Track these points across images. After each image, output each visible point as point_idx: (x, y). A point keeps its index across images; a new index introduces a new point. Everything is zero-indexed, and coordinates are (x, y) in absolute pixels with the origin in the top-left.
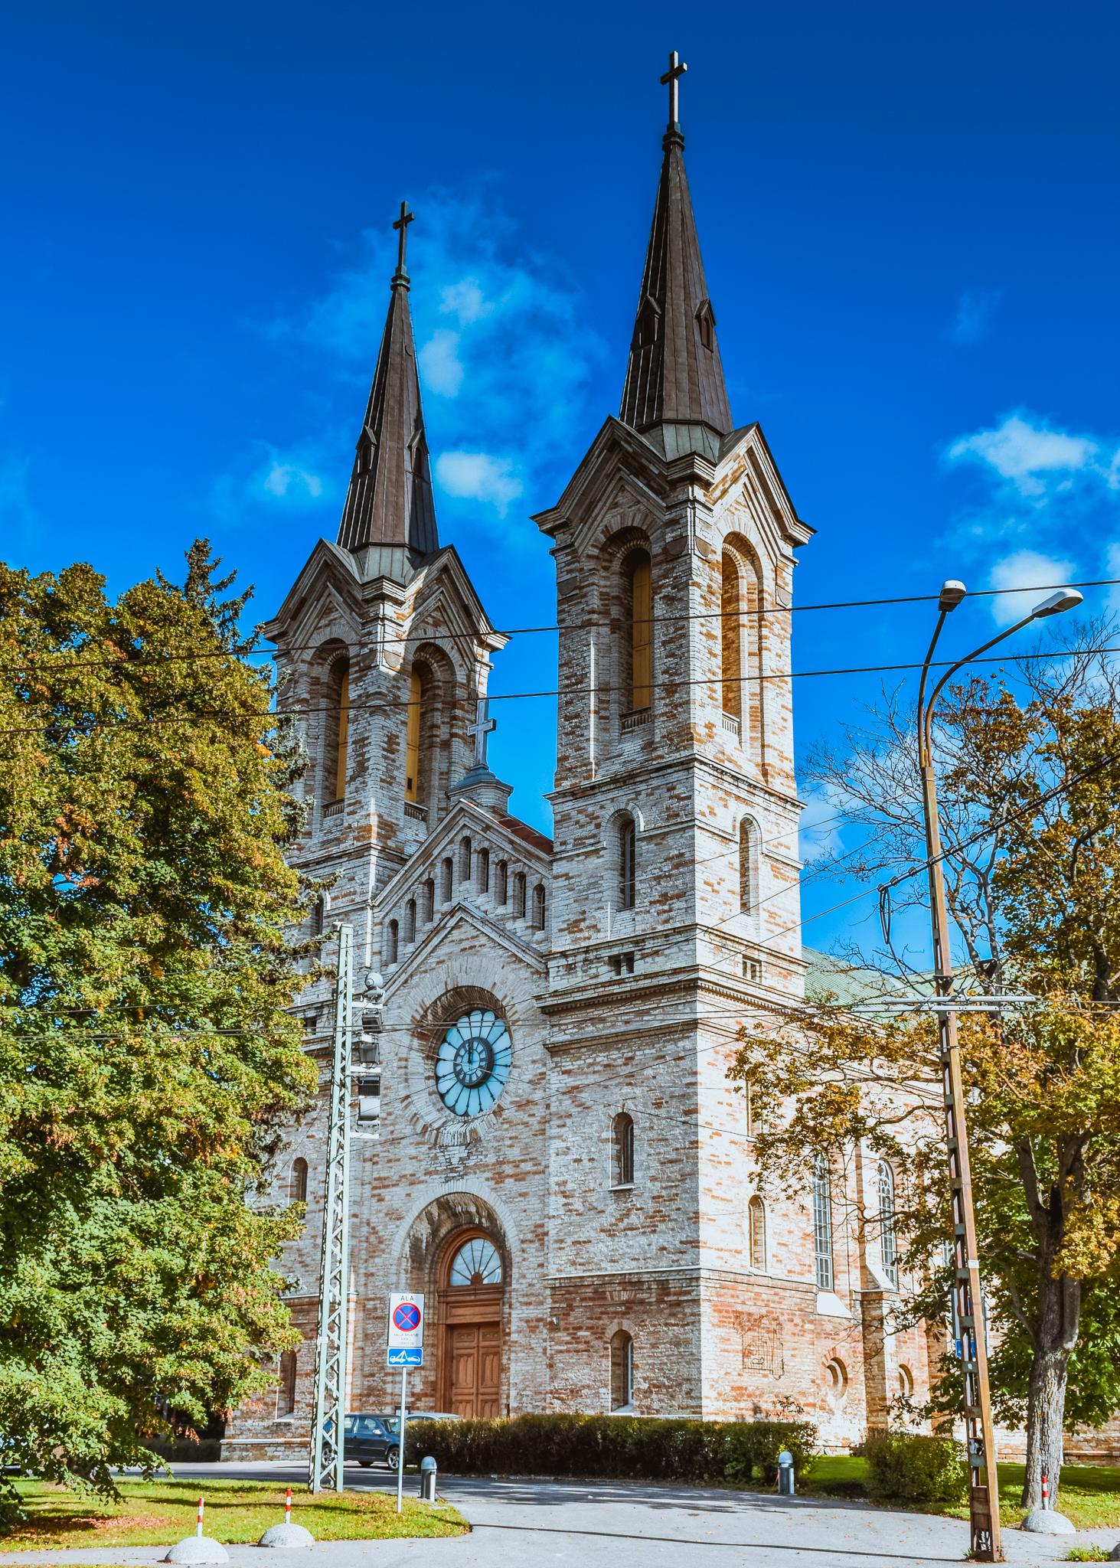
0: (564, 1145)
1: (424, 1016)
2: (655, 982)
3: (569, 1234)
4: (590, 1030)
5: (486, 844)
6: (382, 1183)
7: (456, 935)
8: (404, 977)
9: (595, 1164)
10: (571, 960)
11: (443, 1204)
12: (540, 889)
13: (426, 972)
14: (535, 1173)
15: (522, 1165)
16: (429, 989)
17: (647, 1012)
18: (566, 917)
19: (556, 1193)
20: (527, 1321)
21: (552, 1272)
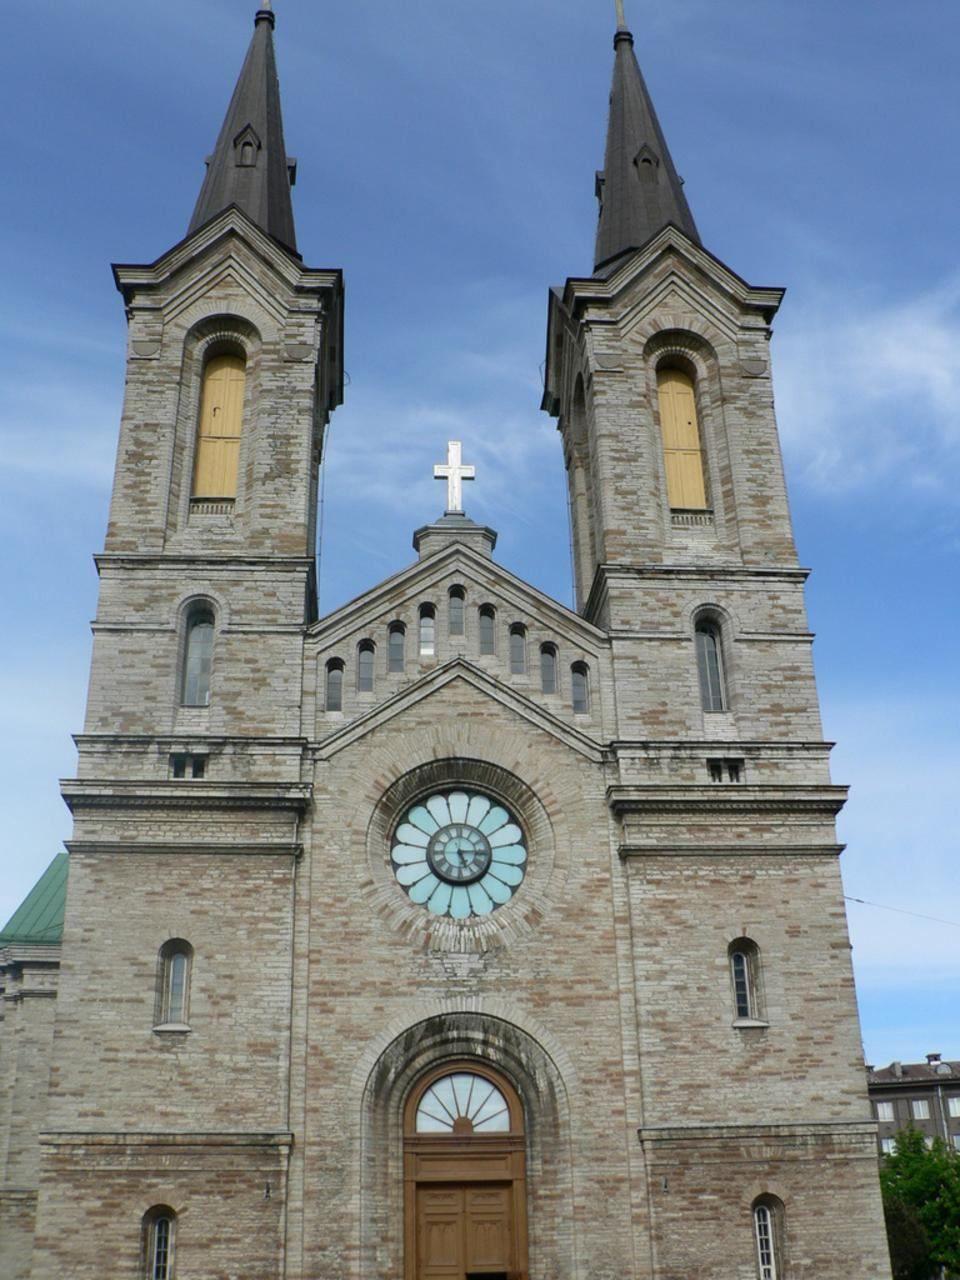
2: (789, 796)
3: (675, 1075)
4: (686, 839)
5: (492, 600)
6: (331, 989)
7: (446, 693)
8: (360, 731)
9: (707, 995)
10: (652, 754)
11: (435, 1026)
12: (580, 668)
13: (398, 730)
14: (599, 998)
15: (578, 987)
16: (410, 752)
17: (768, 829)
19: (648, 1025)
20: (600, 1182)
21: (652, 1118)
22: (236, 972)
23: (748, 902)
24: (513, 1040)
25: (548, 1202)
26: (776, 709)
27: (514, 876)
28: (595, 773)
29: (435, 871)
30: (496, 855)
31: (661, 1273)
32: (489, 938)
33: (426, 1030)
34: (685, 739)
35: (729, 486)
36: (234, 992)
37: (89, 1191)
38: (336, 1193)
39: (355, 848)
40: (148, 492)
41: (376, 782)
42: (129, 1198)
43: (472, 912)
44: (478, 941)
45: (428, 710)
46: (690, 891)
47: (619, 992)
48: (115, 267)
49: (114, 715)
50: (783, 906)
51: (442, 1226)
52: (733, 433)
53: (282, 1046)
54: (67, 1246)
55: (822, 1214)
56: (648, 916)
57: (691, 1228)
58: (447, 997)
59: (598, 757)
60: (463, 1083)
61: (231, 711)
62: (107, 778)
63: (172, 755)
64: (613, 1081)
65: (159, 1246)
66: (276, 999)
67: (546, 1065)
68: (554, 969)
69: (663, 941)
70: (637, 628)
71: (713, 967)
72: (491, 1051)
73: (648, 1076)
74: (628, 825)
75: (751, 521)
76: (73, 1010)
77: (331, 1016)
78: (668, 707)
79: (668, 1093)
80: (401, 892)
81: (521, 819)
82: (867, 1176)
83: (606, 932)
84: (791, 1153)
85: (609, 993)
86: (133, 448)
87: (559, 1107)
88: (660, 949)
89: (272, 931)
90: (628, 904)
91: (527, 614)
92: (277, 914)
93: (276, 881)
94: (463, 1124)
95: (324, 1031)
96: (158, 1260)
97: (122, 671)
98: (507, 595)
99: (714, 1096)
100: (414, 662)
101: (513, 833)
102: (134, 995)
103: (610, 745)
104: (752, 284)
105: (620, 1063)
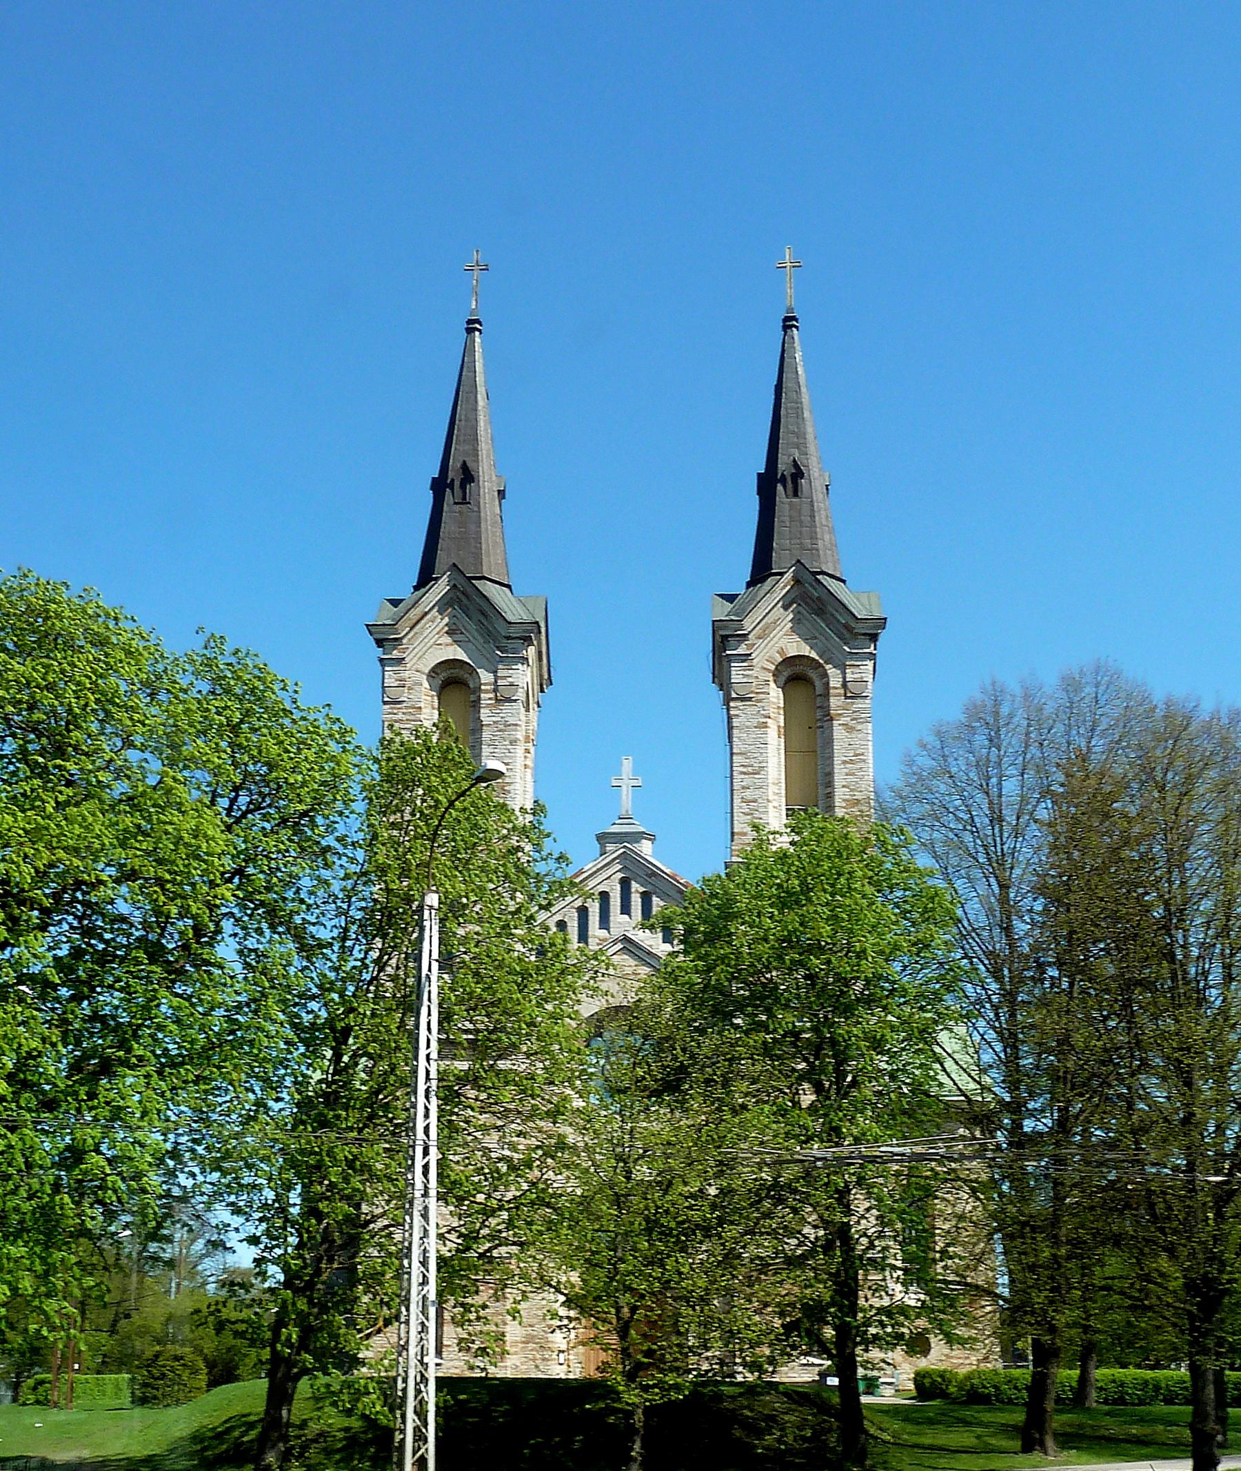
35: (829, 790)
100: (595, 937)
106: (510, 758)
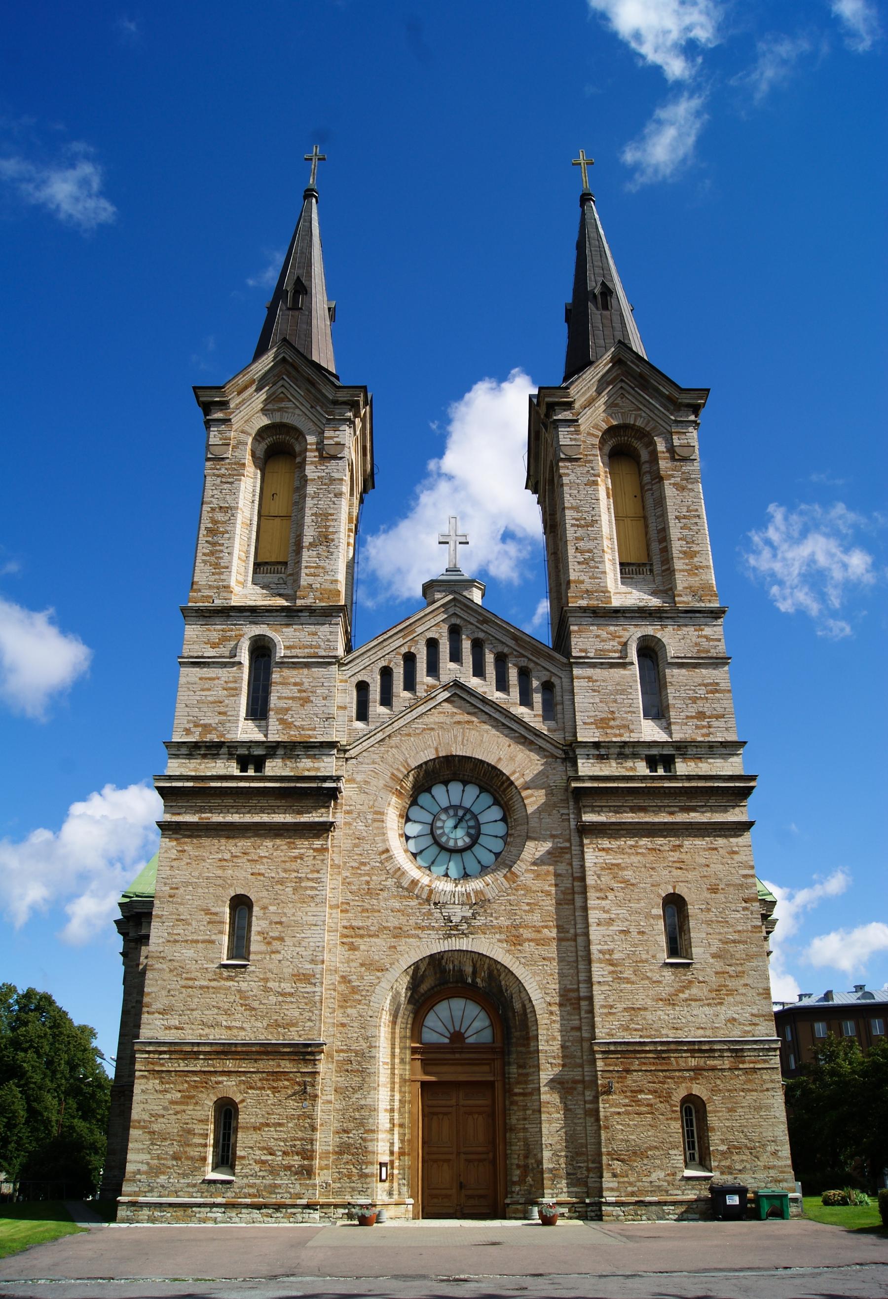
0: (606, 916)
1: (407, 776)
5: (481, 635)
8: (380, 736)
9: (645, 938)
11: (435, 960)
13: (409, 735)
18: (593, 714)
22: (284, 919)
23: (678, 865)
24: (495, 971)
25: (521, 1098)
26: (701, 715)
27: (497, 845)
28: (560, 768)
29: (436, 842)
30: (484, 829)
31: (608, 1155)
32: (476, 892)
33: (429, 964)
34: (628, 740)
35: (664, 544)
36: (283, 935)
37: (172, 1086)
38: (360, 1088)
39: (376, 824)
40: (221, 558)
41: (393, 774)
42: (202, 1092)
43: (465, 873)
44: (468, 895)
45: (430, 720)
46: (633, 857)
47: (576, 935)
48: (195, 388)
49: (195, 726)
50: (706, 868)
51: (441, 1116)
52: (669, 502)
53: (318, 976)
54: (156, 1127)
55: (736, 1111)
56: (599, 876)
57: (633, 1120)
58: (445, 939)
59: (559, 753)
60: (458, 1005)
61: (282, 721)
62: (189, 774)
63: (238, 755)
64: (571, 1004)
65: (225, 1129)
66: (315, 940)
67: (520, 992)
68: (528, 918)
69: (611, 896)
70: (591, 655)
71: (648, 916)
72: (478, 980)
73: (598, 1000)
74: (584, 806)
75: (683, 571)
76: (161, 949)
77: (356, 953)
78: (617, 715)
79: (614, 1014)
80: (412, 857)
81: (502, 802)
82: (772, 1081)
83: (567, 888)
84: (710, 1062)
85: (569, 935)
86: (210, 525)
87: (530, 1024)
88: (608, 902)
89: (312, 888)
90: (583, 867)
91: (507, 646)
92: (316, 875)
93: (315, 850)
94: (457, 1037)
95: (352, 964)
96: (224, 1140)
97: (202, 693)
98: (492, 631)
99: (648, 1015)
101: (495, 813)
102: (207, 937)
103: (570, 745)
104: (683, 387)
105: (578, 990)
106: (336, 509)
